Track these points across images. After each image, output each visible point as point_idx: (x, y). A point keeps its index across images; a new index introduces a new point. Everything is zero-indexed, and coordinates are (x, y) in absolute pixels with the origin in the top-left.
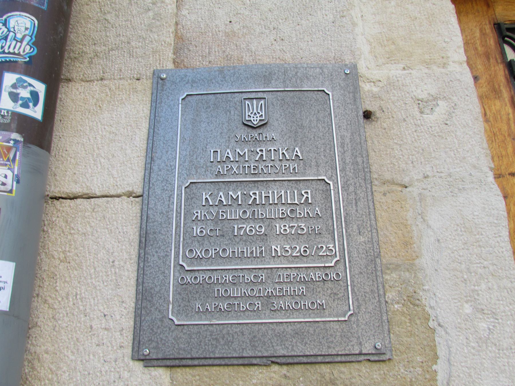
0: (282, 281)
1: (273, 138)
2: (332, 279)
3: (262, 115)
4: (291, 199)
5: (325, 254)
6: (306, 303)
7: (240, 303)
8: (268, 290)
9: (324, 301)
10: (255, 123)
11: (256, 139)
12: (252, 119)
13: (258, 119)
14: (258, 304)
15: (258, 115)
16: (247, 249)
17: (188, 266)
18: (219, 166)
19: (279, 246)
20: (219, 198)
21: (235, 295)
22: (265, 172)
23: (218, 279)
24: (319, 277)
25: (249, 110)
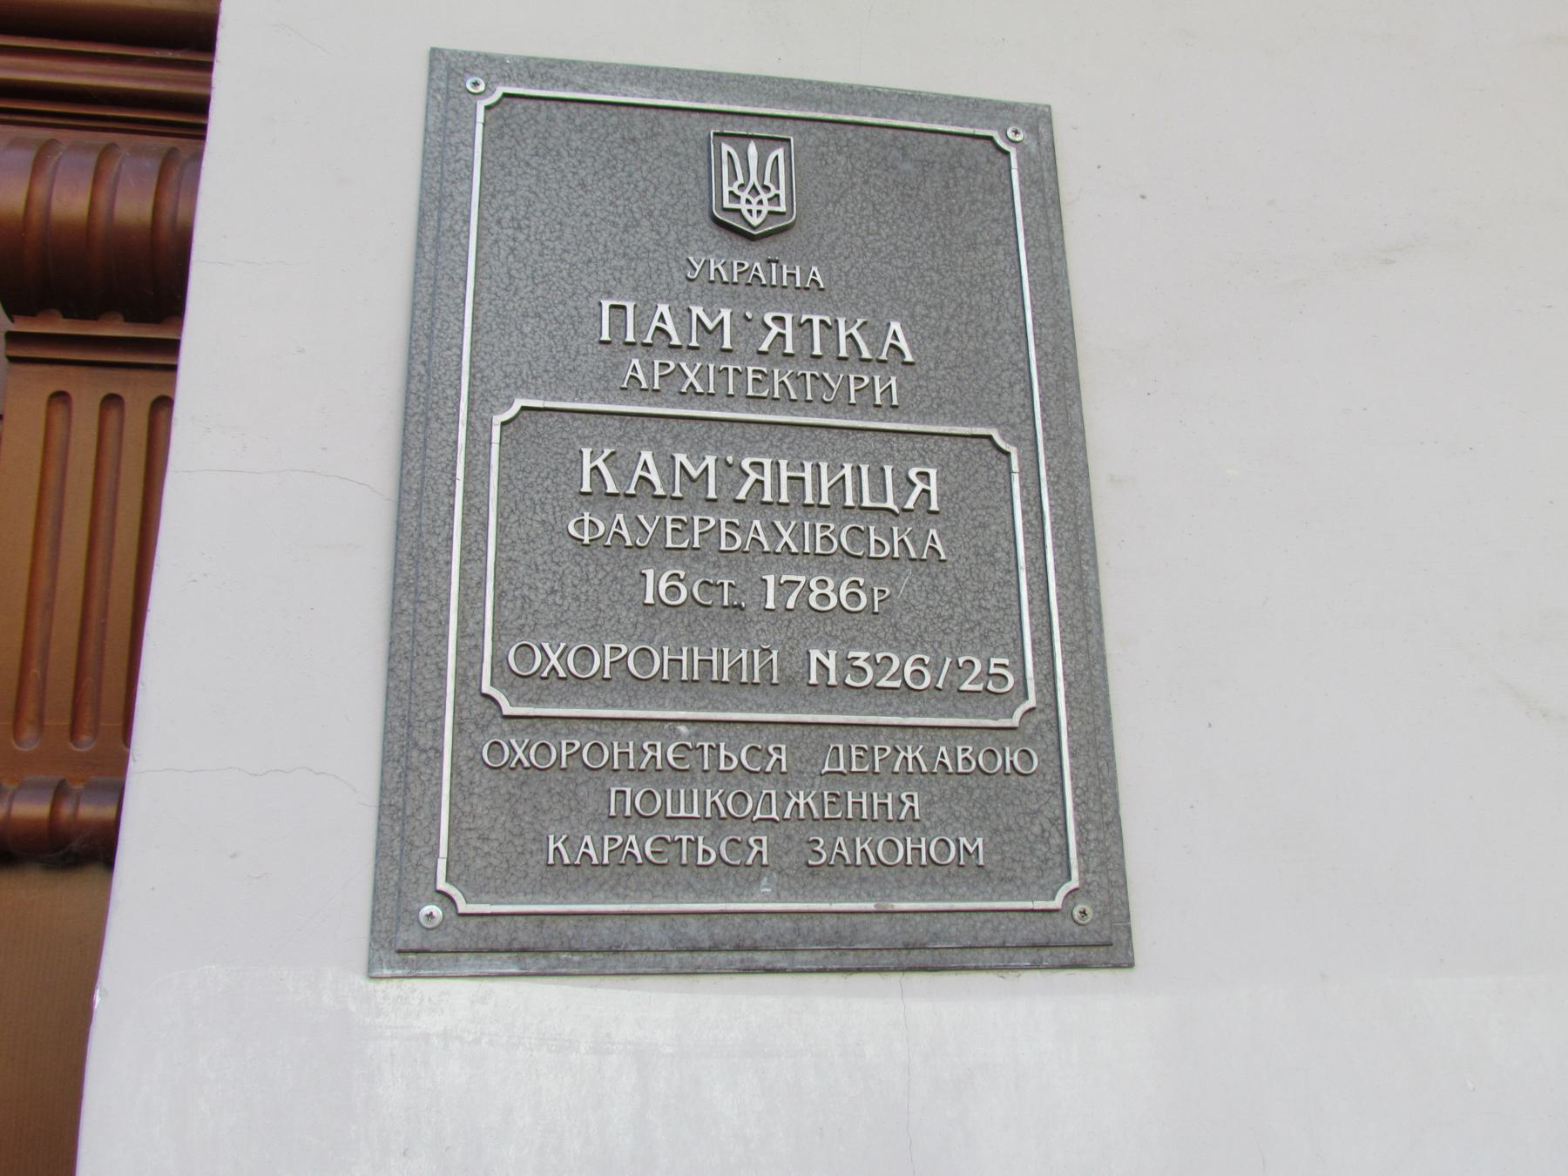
4: (873, 498)
5: (979, 687)
6: (923, 846)
7: (697, 839)
8: (794, 799)
9: (979, 841)
10: (755, 221)
12: (744, 207)
13: (766, 208)
14: (761, 845)
15: (764, 196)
21: (682, 813)
23: (624, 754)
25: (733, 176)
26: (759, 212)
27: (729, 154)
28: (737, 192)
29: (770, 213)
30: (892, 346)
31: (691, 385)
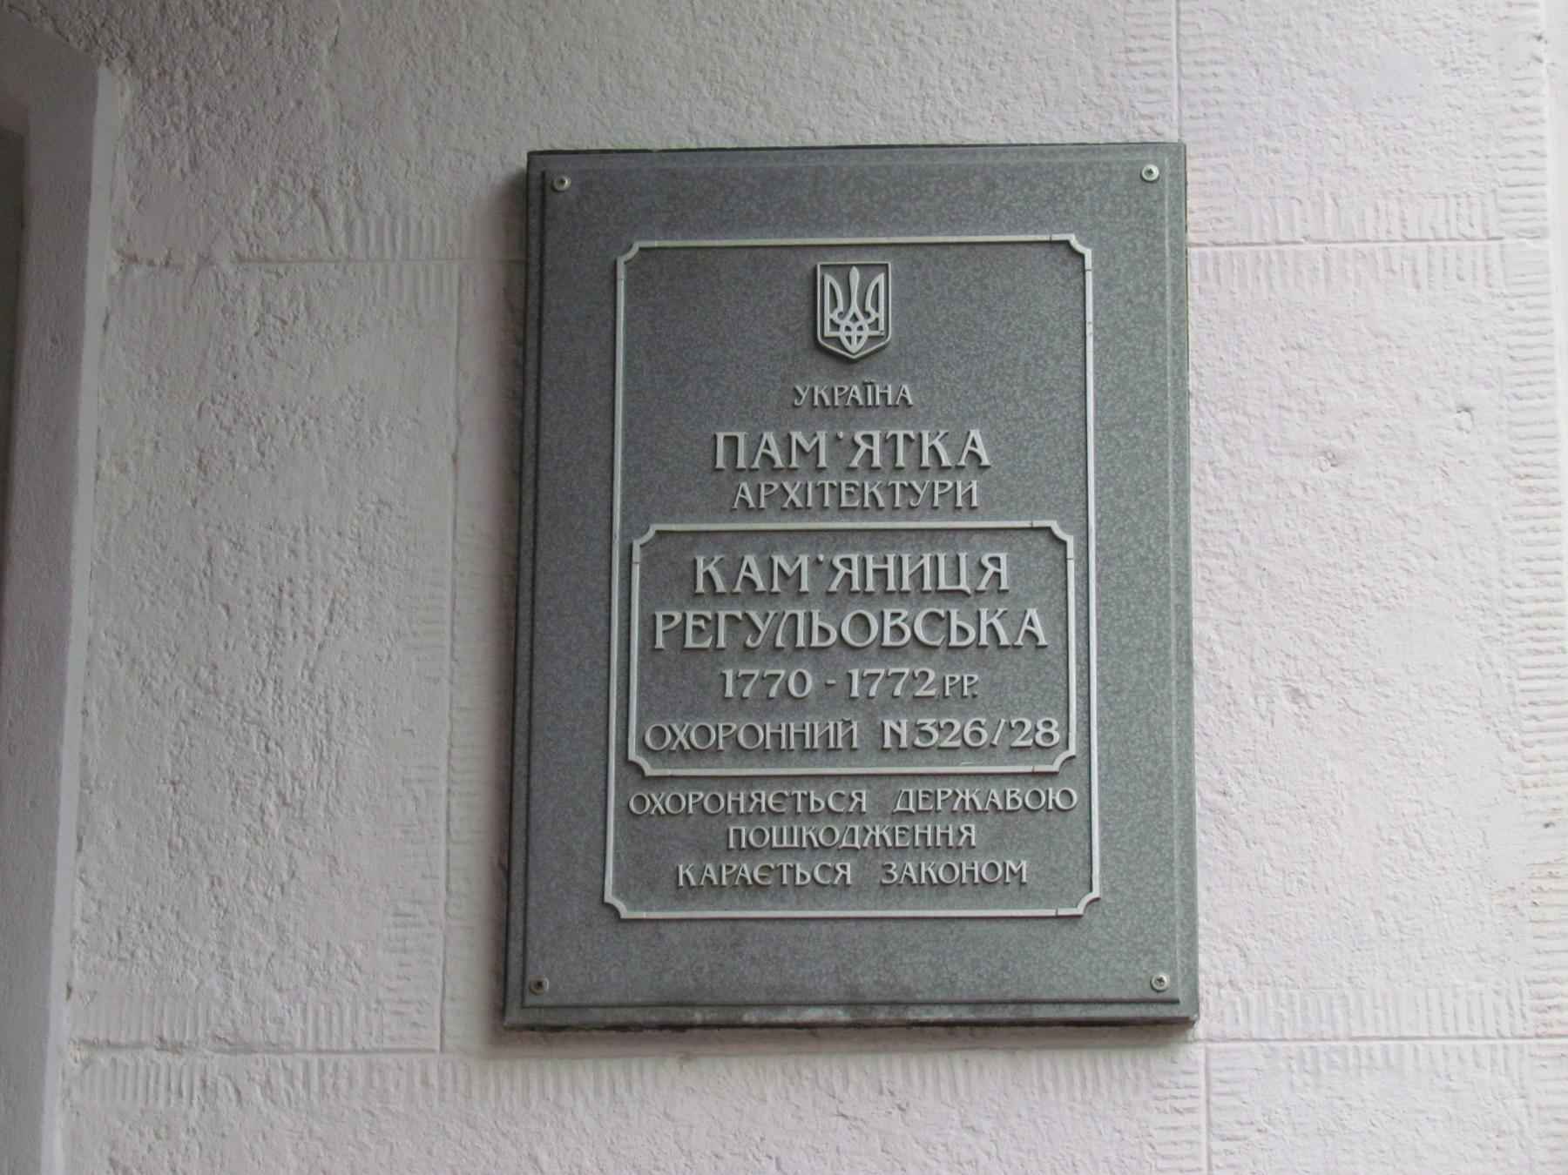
0: (911, 808)
1: (904, 400)
2: (1051, 807)
8: (871, 832)
10: (854, 347)
11: (855, 401)
12: (842, 334)
13: (867, 332)
15: (862, 321)
17: (653, 766)
18: (744, 485)
21: (785, 844)
22: (881, 504)
24: (1015, 801)
26: (859, 338)
27: (831, 286)
29: (870, 337)
31: (792, 501)
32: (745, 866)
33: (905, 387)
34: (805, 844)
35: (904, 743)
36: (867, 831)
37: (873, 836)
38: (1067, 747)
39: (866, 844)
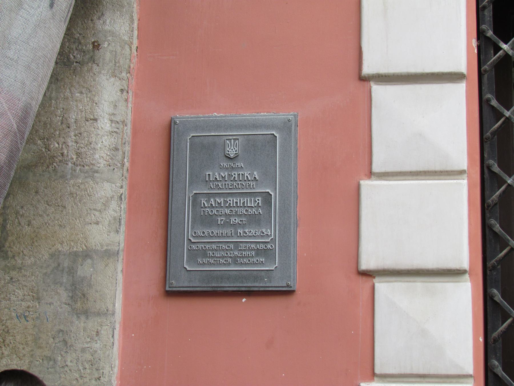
2: (269, 248)
3: (236, 150)
10: (232, 156)
11: (232, 167)
12: (230, 153)
13: (235, 152)
15: (234, 150)
16: (224, 231)
18: (211, 184)
19: (242, 231)
20: (211, 203)
21: (218, 256)
22: (237, 187)
24: (262, 247)
26: (233, 154)
28: (229, 150)
29: (235, 154)
30: (254, 177)
32: (210, 260)
33: (242, 164)
34: (222, 256)
35: (242, 235)
36: (234, 253)
37: (235, 254)
38: (271, 237)
39: (234, 256)
